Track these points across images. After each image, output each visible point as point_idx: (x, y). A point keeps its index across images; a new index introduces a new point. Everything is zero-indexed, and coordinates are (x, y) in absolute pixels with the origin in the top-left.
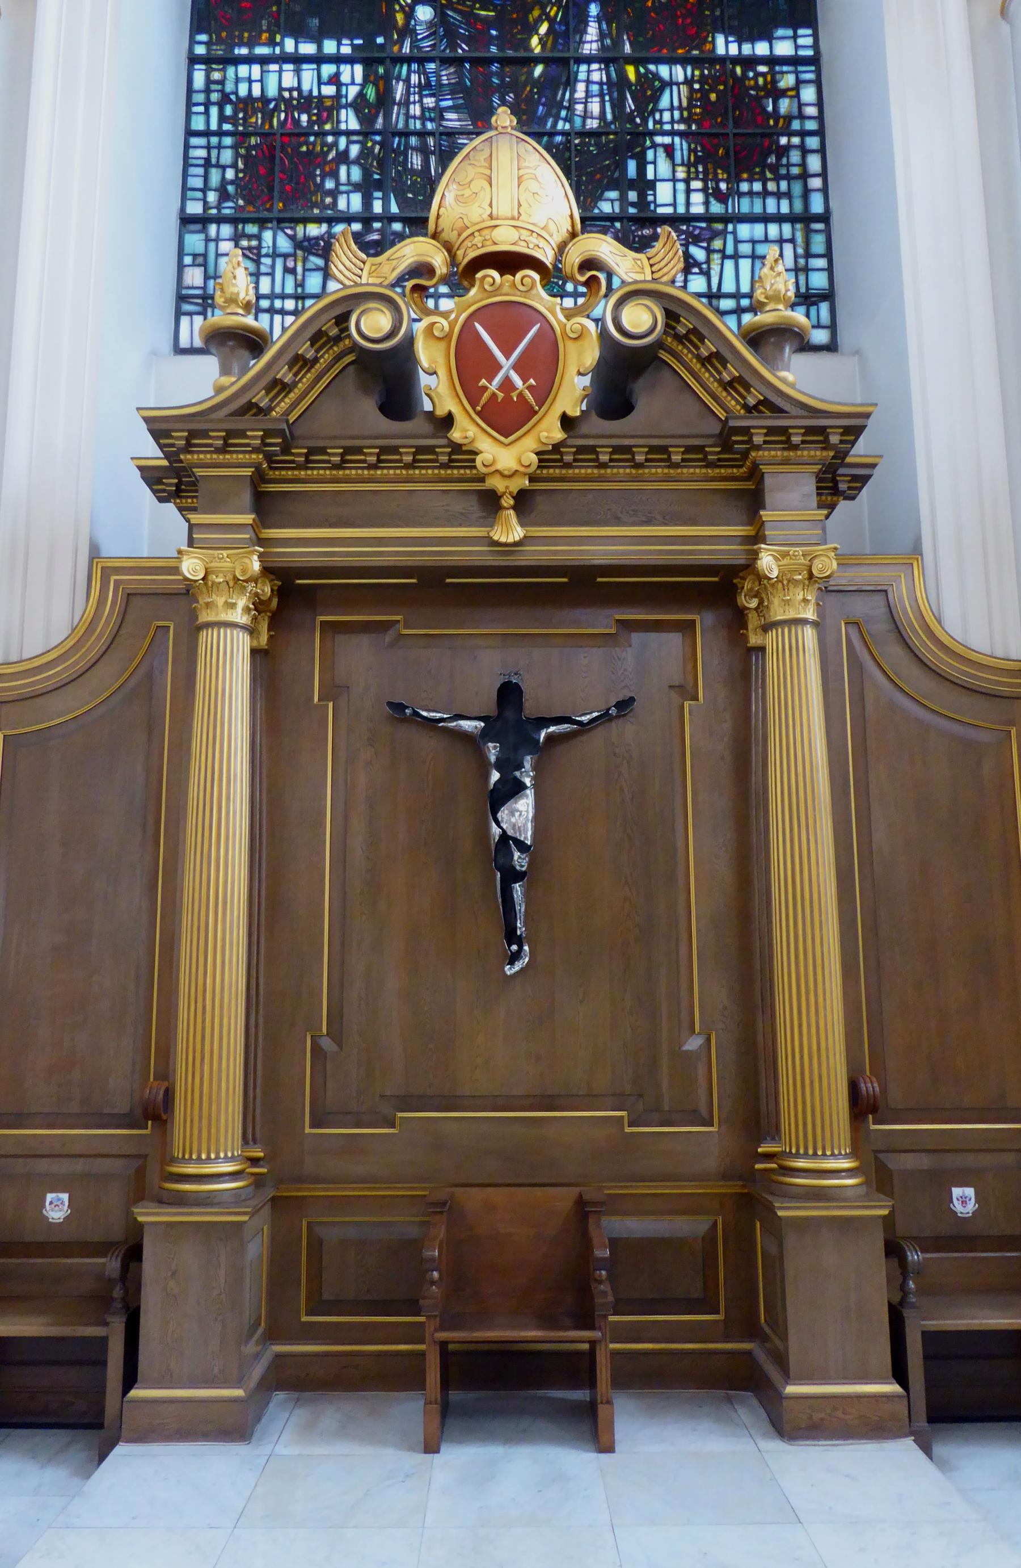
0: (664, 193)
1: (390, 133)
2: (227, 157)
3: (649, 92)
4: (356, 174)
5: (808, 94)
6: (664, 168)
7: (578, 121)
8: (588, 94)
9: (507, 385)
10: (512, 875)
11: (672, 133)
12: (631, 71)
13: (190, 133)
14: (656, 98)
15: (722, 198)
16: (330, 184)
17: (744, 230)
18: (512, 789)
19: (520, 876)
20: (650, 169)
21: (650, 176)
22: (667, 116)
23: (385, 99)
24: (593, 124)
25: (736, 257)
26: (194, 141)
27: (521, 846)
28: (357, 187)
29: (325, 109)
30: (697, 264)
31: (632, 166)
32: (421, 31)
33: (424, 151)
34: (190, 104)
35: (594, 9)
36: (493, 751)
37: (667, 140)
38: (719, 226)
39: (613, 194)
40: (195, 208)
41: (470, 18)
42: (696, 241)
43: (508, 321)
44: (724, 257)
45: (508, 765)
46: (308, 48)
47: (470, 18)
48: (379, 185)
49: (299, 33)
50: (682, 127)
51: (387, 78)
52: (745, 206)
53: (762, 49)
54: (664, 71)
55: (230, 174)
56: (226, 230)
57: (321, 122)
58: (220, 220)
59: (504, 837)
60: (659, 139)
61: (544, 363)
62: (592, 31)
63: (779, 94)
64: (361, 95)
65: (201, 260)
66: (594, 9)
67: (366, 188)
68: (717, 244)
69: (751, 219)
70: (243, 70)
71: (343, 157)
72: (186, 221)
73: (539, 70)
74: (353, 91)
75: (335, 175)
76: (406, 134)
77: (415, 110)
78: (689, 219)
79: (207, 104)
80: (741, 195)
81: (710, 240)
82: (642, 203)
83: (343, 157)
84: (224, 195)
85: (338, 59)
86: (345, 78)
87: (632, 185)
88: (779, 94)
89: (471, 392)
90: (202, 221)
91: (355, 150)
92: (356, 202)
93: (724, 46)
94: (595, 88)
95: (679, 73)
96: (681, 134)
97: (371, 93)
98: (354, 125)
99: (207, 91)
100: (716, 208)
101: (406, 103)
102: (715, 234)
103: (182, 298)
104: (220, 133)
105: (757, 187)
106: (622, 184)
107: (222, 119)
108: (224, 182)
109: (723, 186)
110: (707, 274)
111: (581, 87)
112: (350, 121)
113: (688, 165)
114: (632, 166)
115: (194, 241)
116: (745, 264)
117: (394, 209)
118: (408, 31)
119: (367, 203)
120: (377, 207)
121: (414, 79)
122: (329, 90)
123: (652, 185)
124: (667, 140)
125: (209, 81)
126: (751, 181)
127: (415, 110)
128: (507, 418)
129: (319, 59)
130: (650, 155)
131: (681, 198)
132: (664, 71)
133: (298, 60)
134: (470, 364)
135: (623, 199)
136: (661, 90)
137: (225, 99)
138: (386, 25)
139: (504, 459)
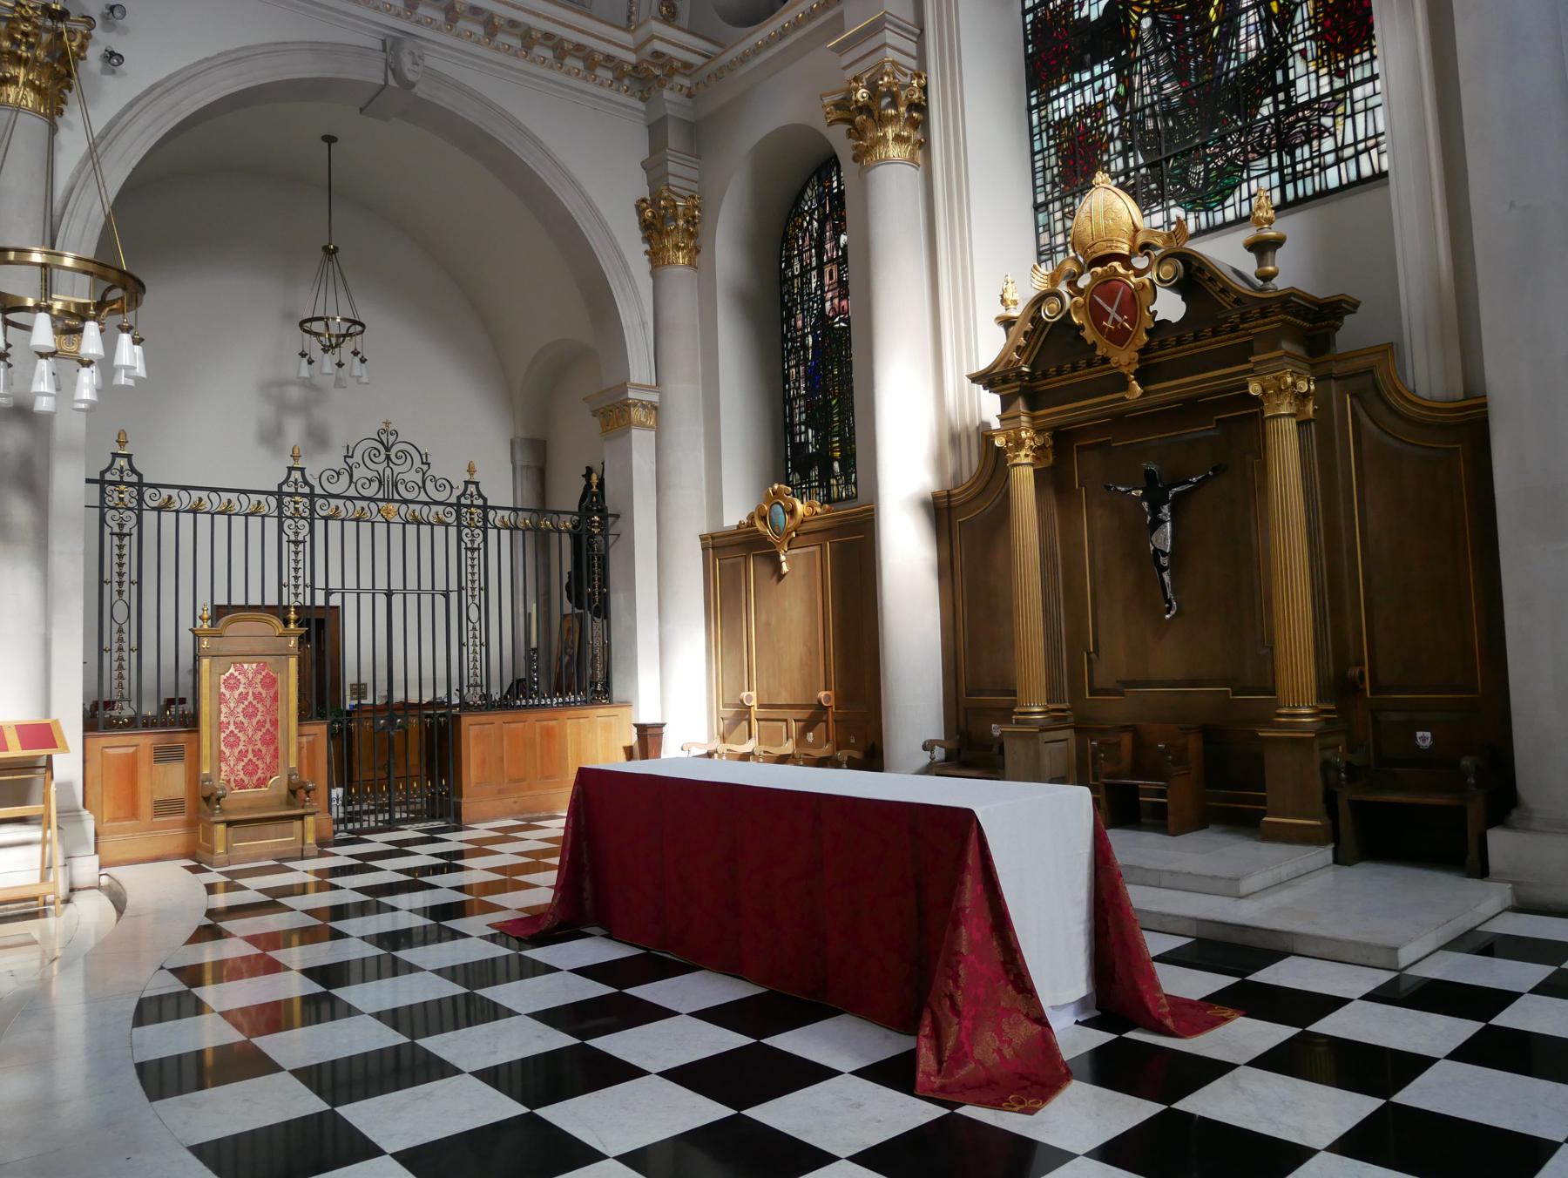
0: (1301, 85)
1: (1134, 111)
2: (1053, 160)
4: (1118, 145)
6: (1300, 67)
7: (1242, 56)
8: (1248, 35)
9: (1115, 322)
10: (1162, 569)
11: (1304, 40)
13: (1033, 154)
14: (1292, 18)
15: (1342, 74)
16: (1105, 158)
17: (1358, 93)
18: (1157, 523)
19: (1164, 569)
20: (1291, 72)
21: (1292, 77)
22: (1300, 28)
23: (1130, 91)
24: (1252, 55)
25: (1353, 115)
26: (1037, 157)
27: (1164, 554)
28: (1119, 154)
29: (1096, 111)
30: (1327, 130)
31: (1279, 74)
32: (1145, 36)
33: (1154, 116)
34: (1032, 135)
37: (1301, 46)
38: (1341, 96)
39: (1269, 100)
40: (1041, 198)
41: (1172, 14)
42: (1325, 112)
44: (1346, 118)
45: (1155, 510)
46: (1087, 76)
48: (1131, 148)
49: (1080, 70)
50: (1311, 32)
51: (1130, 77)
52: (1357, 74)
55: (1056, 171)
56: (1057, 205)
57: (1097, 120)
58: (1053, 201)
59: (1156, 550)
60: (1296, 48)
64: (1117, 93)
65: (1047, 227)
67: (1124, 154)
68: (1340, 110)
69: (1363, 81)
70: (1056, 104)
71: (1111, 138)
72: (1037, 207)
75: (1107, 150)
76: (1143, 108)
77: (1147, 90)
78: (1319, 98)
79: (1040, 133)
80: (1354, 66)
81: (1334, 109)
82: (1288, 100)
83: (1111, 138)
84: (1054, 185)
85: (1103, 76)
86: (1107, 86)
87: (1279, 89)
89: (1101, 329)
90: (1046, 204)
91: (1116, 130)
92: (1120, 161)
94: (1252, 28)
96: (1310, 38)
97: (1122, 90)
98: (1115, 115)
99: (1040, 124)
100: (1338, 83)
101: (1141, 88)
102: (1339, 102)
103: (1040, 254)
104: (1049, 148)
105: (1366, 55)
107: (1049, 139)
108: (1053, 177)
109: (1342, 65)
110: (1334, 135)
111: (1243, 31)
112: (1112, 113)
113: (1316, 59)
114: (1279, 74)
115: (1042, 217)
116: (1360, 118)
117: (1141, 161)
118: (1139, 39)
119: (1126, 162)
120: (1132, 163)
121: (1144, 70)
122: (1099, 98)
123: (1293, 84)
124: (1301, 46)
125: (1040, 118)
126: (1361, 53)
127: (1147, 90)
128: (1119, 337)
129: (1093, 80)
130: (1291, 62)
131: (1313, 85)
133: (1082, 85)
135: (1276, 103)
136: (1295, 11)
137: (1049, 126)
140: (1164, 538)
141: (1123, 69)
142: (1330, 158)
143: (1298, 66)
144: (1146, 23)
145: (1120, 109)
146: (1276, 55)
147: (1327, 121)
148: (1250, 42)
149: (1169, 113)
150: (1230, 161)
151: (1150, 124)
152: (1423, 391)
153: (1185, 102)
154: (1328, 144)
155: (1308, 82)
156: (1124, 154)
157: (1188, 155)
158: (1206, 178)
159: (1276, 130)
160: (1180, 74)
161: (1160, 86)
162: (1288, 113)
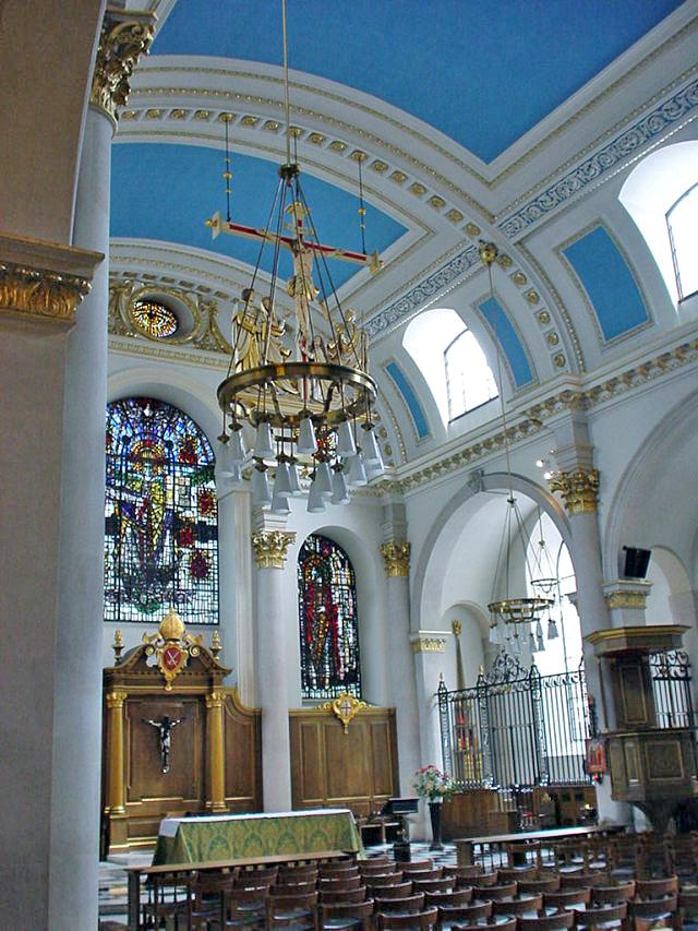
0: (182, 583)
3: (180, 555)
5: (215, 558)
12: (176, 550)
17: (201, 593)
18: (166, 737)
35: (168, 532)
36: (163, 730)
43: (173, 650)
47: (139, 532)
53: (205, 546)
54: (183, 550)
61: (178, 659)
62: (168, 537)
63: (209, 558)
66: (168, 532)
67: (115, 577)
73: (155, 548)
74: (111, 551)
82: (178, 586)
88: (209, 558)
91: (112, 567)
93: (198, 544)
95: (187, 551)
97: (116, 552)
106: (174, 580)
118: (124, 535)
128: (171, 668)
132: (183, 550)
134: (166, 658)
138: (120, 533)
139: (169, 675)
140: (167, 742)
141: (117, 542)
142: (190, 612)
143: (182, 576)
144: (129, 530)
145: (115, 559)
146: (175, 569)
147: (190, 598)
148: (166, 558)
149: (133, 570)
150: (157, 598)
151: (126, 571)
152: (242, 703)
153: (142, 567)
154: (189, 607)
155: (184, 580)
156: (115, 577)
157: (142, 591)
158: (147, 603)
159: (173, 593)
160: (140, 558)
161: (132, 558)
162: (178, 590)
